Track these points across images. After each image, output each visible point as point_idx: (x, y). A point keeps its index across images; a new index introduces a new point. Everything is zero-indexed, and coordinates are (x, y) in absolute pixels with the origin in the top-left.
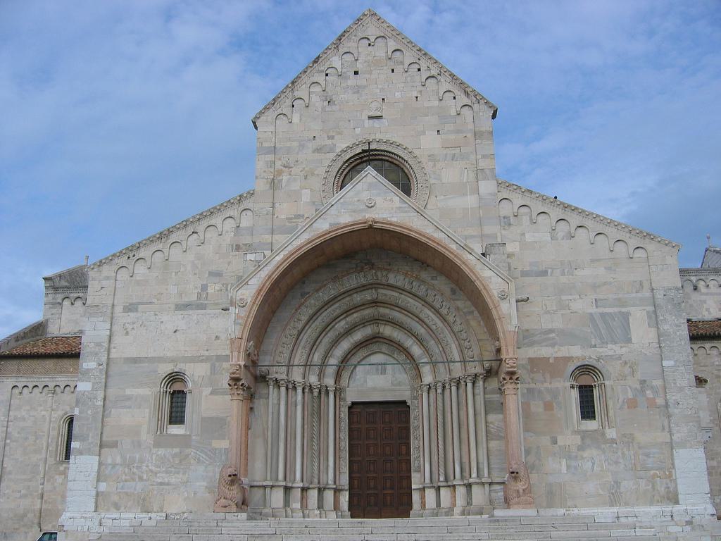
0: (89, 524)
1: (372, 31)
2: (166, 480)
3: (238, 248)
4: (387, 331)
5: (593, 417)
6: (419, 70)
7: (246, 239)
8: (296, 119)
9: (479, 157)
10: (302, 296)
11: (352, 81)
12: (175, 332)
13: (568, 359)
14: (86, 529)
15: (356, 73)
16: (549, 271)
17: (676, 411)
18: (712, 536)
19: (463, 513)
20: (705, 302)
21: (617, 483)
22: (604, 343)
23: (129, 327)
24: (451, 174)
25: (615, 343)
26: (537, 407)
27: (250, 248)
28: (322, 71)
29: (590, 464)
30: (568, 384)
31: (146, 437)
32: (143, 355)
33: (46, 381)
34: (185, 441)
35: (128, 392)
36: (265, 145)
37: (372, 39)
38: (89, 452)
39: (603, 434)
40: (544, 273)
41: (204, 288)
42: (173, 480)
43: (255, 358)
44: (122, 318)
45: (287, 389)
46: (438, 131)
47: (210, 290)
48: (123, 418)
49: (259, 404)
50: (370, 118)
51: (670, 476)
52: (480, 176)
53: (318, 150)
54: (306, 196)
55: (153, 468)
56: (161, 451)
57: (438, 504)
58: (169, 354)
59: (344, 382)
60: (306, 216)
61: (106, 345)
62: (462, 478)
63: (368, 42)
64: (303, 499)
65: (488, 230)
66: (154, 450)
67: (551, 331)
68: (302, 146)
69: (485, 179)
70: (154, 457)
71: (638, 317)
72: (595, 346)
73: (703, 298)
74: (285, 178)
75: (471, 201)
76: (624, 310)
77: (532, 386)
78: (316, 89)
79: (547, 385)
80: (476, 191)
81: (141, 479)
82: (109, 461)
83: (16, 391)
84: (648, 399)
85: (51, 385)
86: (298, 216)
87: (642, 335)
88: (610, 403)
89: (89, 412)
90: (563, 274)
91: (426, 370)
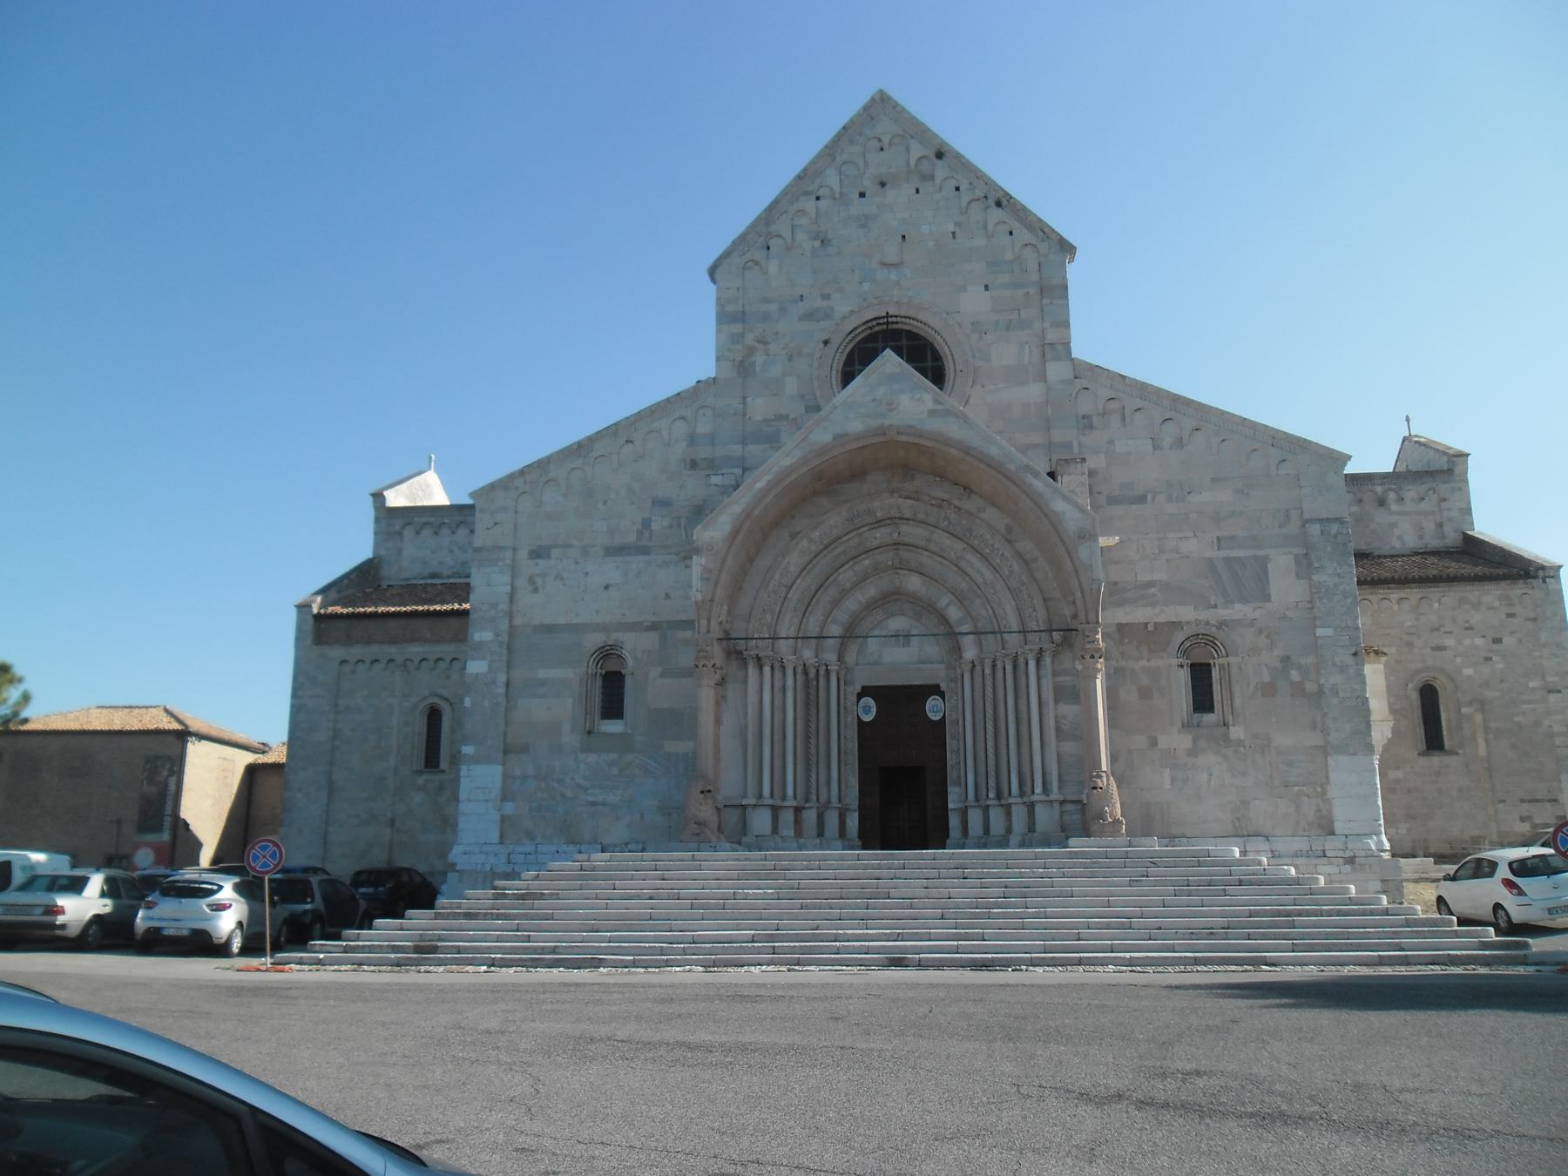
0: (492, 860)
1: (885, 128)
2: (600, 799)
3: (694, 464)
4: (914, 583)
5: (1211, 709)
6: (957, 189)
7: (703, 452)
8: (773, 267)
9: (1047, 325)
10: (793, 536)
11: (857, 208)
12: (606, 587)
13: (1176, 625)
14: (488, 868)
15: (862, 195)
16: (1149, 497)
17: (1335, 700)
18: (1383, 881)
19: (1022, 845)
20: (1395, 525)
21: (1245, 803)
23: (539, 581)
25: (1244, 600)
26: (1129, 694)
27: (712, 465)
28: (808, 193)
29: (1205, 776)
30: (1175, 661)
31: (570, 737)
32: (561, 621)
33: (391, 650)
34: (624, 743)
35: (542, 674)
36: (730, 308)
37: (886, 140)
38: (488, 760)
39: (1226, 737)
40: (1141, 499)
41: (646, 524)
42: (611, 798)
43: (728, 626)
45: (772, 667)
46: (986, 288)
47: (655, 526)
48: (535, 709)
49: (732, 691)
50: (884, 265)
51: (1324, 793)
52: (1049, 355)
53: (808, 316)
54: (791, 386)
55: (582, 782)
56: (592, 758)
57: (987, 830)
58: (598, 620)
59: (850, 658)
60: (792, 416)
61: (504, 606)
62: (1022, 794)
63: (878, 145)
64: (798, 822)
65: (1057, 436)
66: (582, 756)
67: (1151, 584)
68: (783, 310)
69: (1056, 358)
70: (582, 766)
71: (1281, 563)
72: (1215, 606)
73: (1393, 519)
74: (759, 359)
76: (1259, 553)
77: (1122, 663)
78: (803, 221)
79: (1143, 663)
80: (1042, 377)
81: (563, 796)
82: (517, 772)
83: (347, 668)
84: (1292, 683)
85: (399, 659)
86: (780, 417)
87: (1285, 587)
88: (1237, 690)
89: (486, 703)
90: (1170, 500)
91: (968, 642)
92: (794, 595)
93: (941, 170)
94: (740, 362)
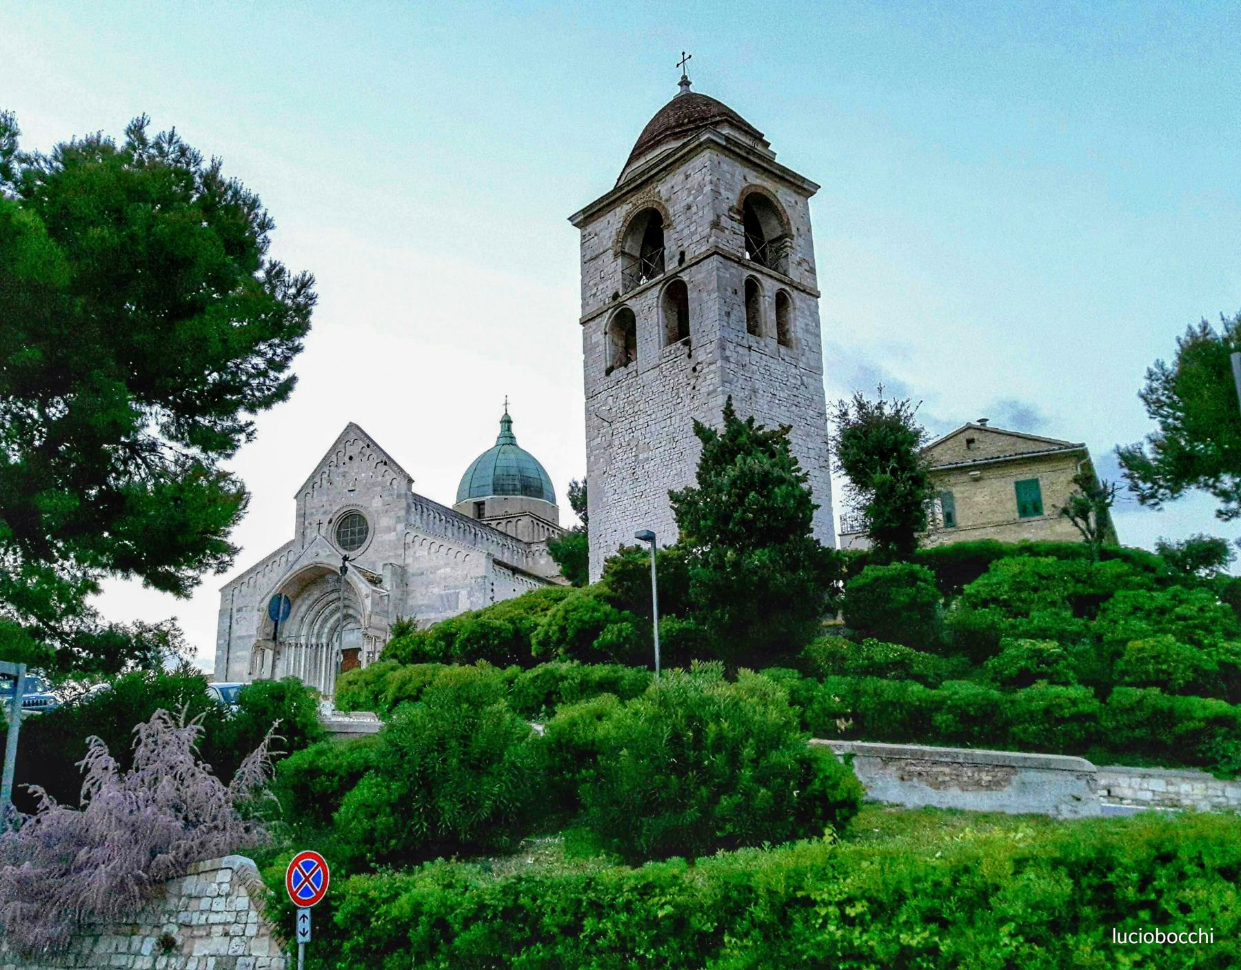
1: (352, 436)
4: (351, 612)
13: (428, 620)
22: (445, 610)
24: (385, 522)
44: (235, 616)
71: (463, 593)
75: (392, 536)
80: (395, 530)
92: (307, 620)
93: (368, 451)
94: (302, 532)
